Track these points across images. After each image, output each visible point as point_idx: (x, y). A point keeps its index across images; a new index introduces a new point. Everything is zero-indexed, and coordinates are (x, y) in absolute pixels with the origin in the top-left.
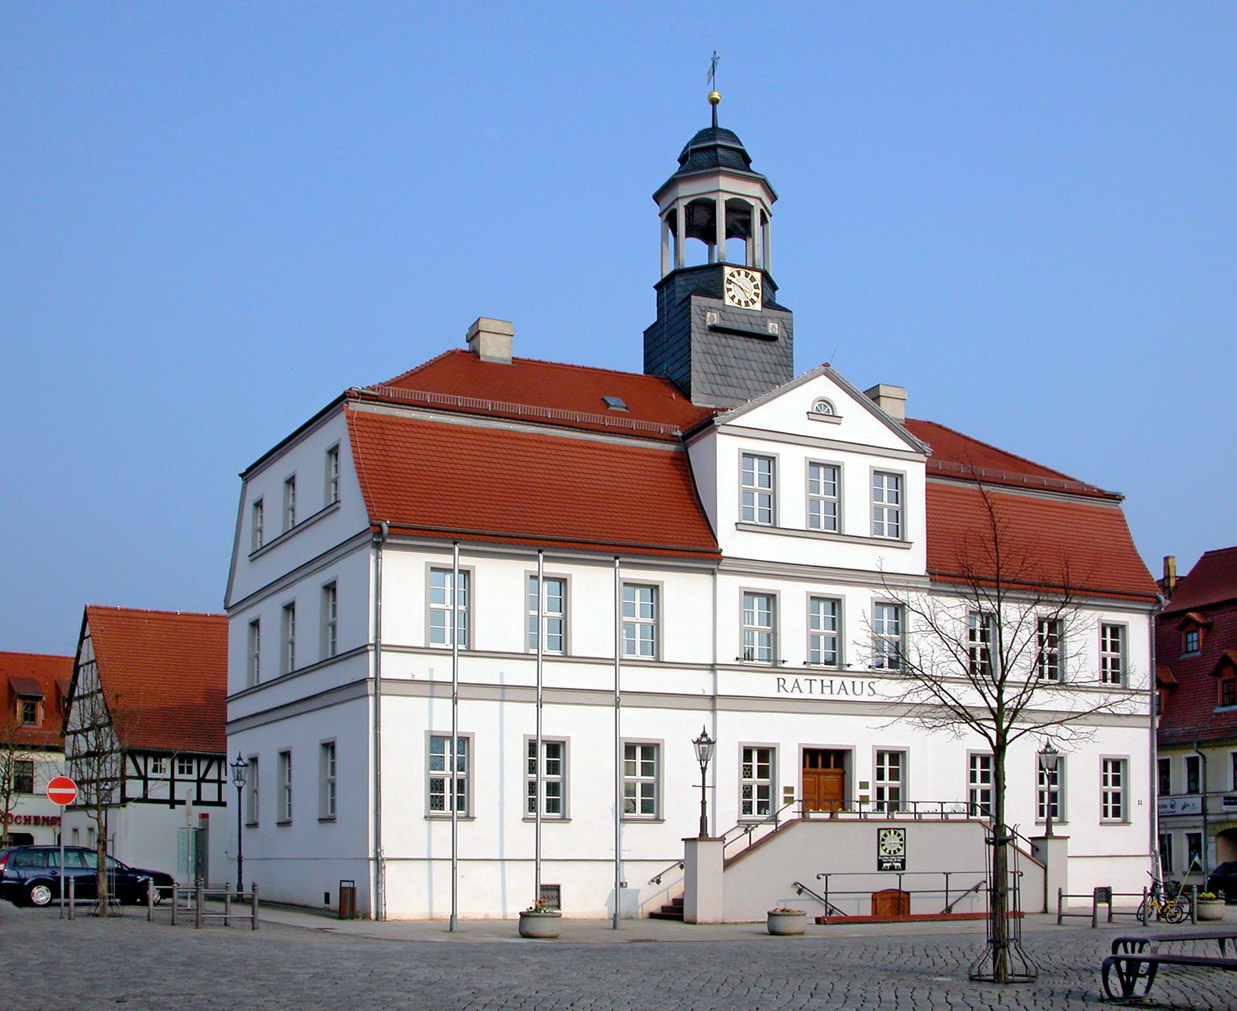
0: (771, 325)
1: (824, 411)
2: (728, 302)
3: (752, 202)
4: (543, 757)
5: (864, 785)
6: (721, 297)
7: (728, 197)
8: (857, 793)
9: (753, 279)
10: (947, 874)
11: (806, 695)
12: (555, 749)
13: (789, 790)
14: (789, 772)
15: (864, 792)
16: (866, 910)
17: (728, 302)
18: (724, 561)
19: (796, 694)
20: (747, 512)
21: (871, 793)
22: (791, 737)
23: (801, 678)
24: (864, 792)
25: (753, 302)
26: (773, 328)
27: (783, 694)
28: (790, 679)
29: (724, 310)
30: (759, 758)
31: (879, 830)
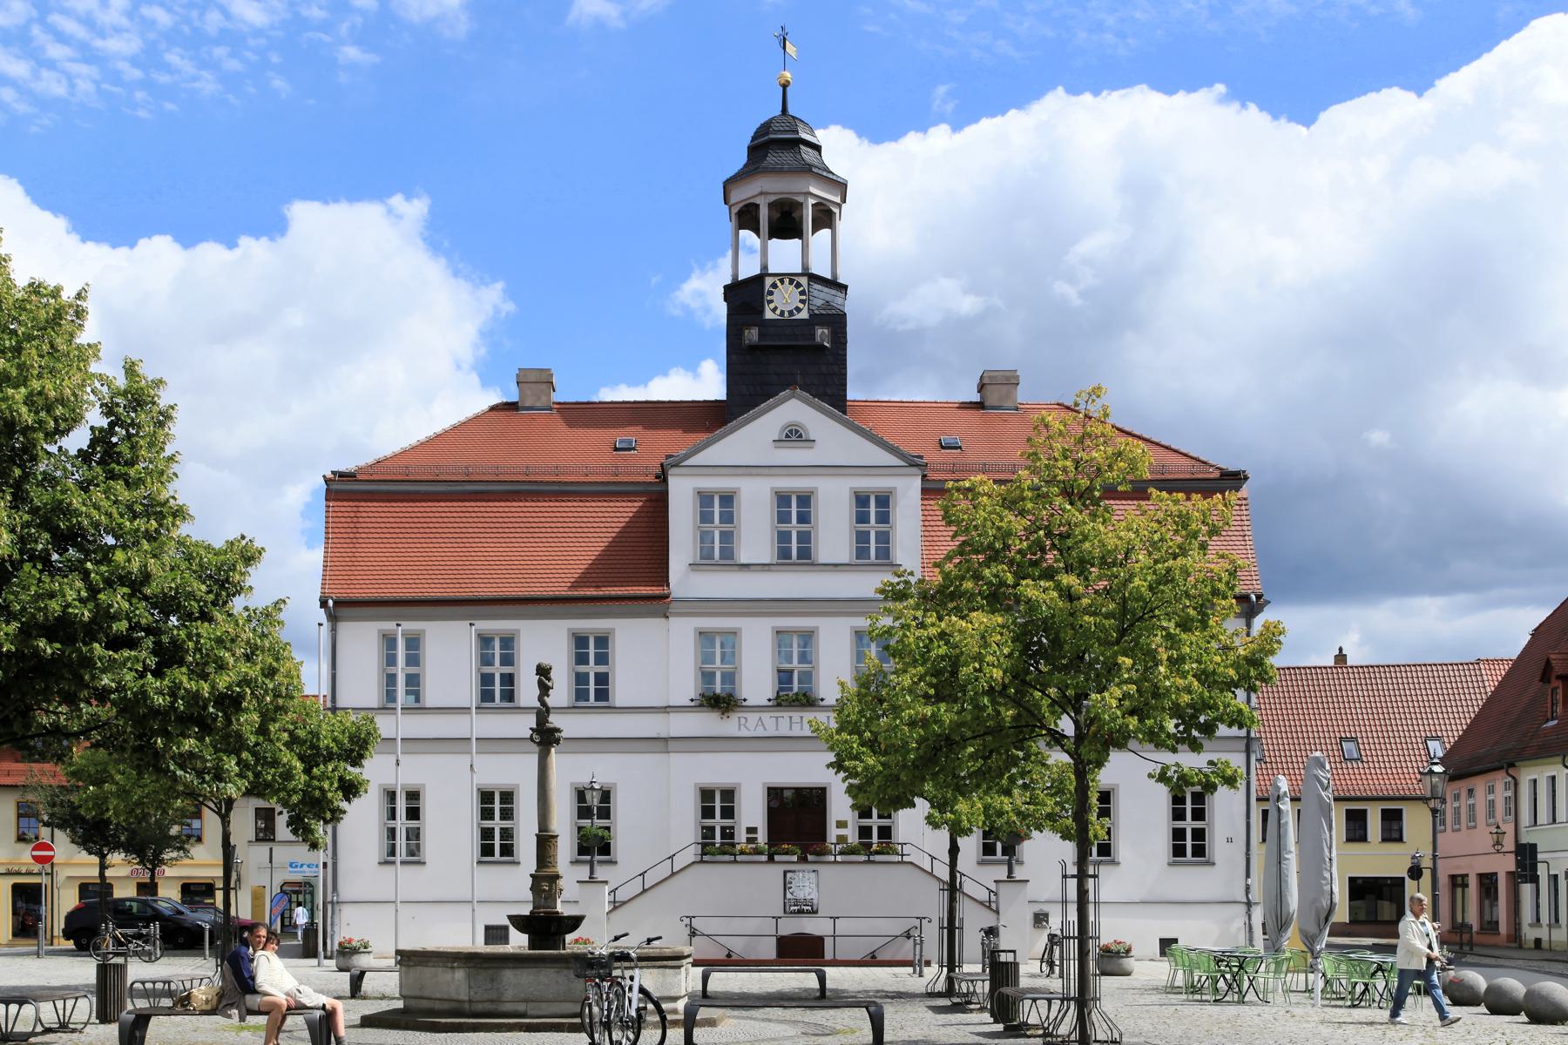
0: (820, 331)
1: (794, 435)
2: (769, 315)
3: (800, 199)
4: (401, 805)
5: (841, 824)
6: (762, 312)
7: (773, 198)
8: (833, 833)
9: (798, 285)
10: (834, 918)
11: (771, 732)
12: (413, 796)
13: (752, 830)
14: (752, 813)
15: (842, 832)
16: (769, 950)
17: (769, 315)
18: (673, 605)
19: (760, 732)
20: (706, 554)
21: (852, 837)
22: (753, 779)
23: (766, 716)
24: (842, 832)
25: (799, 310)
26: (822, 334)
27: (744, 733)
28: (753, 718)
29: (765, 325)
30: (716, 803)
31: (785, 873)
